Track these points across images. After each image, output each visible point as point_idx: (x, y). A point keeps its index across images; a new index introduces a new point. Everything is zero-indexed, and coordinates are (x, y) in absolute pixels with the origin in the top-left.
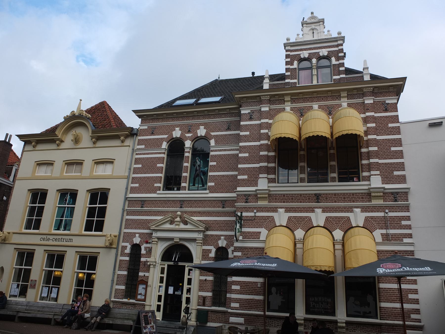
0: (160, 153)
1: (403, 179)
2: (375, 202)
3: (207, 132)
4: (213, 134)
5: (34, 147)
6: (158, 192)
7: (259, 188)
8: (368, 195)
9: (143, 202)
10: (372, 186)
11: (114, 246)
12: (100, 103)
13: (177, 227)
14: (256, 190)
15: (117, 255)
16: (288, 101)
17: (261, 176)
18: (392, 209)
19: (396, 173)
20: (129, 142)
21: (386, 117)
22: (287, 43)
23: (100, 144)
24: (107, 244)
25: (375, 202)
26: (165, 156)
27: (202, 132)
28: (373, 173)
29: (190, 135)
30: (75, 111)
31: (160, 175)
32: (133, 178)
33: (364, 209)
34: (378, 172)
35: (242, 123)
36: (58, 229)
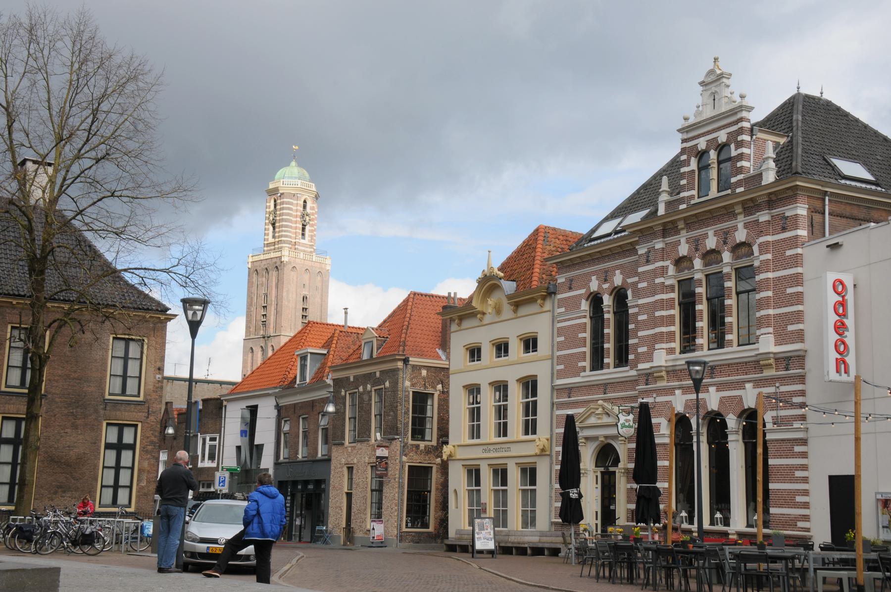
0: (580, 318)
1: (799, 336)
2: (767, 373)
3: (623, 279)
4: (630, 281)
5: (459, 325)
6: (582, 374)
7: (655, 364)
8: (757, 364)
9: (569, 390)
10: (761, 351)
11: (548, 453)
12: (524, 242)
13: (599, 421)
14: (652, 367)
15: (551, 464)
16: (683, 229)
17: (657, 346)
18: (783, 380)
19: (791, 328)
20: (548, 305)
21: (784, 240)
22: (683, 129)
23: (523, 311)
24: (538, 452)
25: (767, 373)
26: (587, 321)
27: (618, 280)
28: (763, 330)
29: (606, 286)
30: (486, 269)
31: (583, 349)
32: (558, 357)
33: (758, 383)
34: (771, 330)
35: (640, 270)
36: (500, 436)
